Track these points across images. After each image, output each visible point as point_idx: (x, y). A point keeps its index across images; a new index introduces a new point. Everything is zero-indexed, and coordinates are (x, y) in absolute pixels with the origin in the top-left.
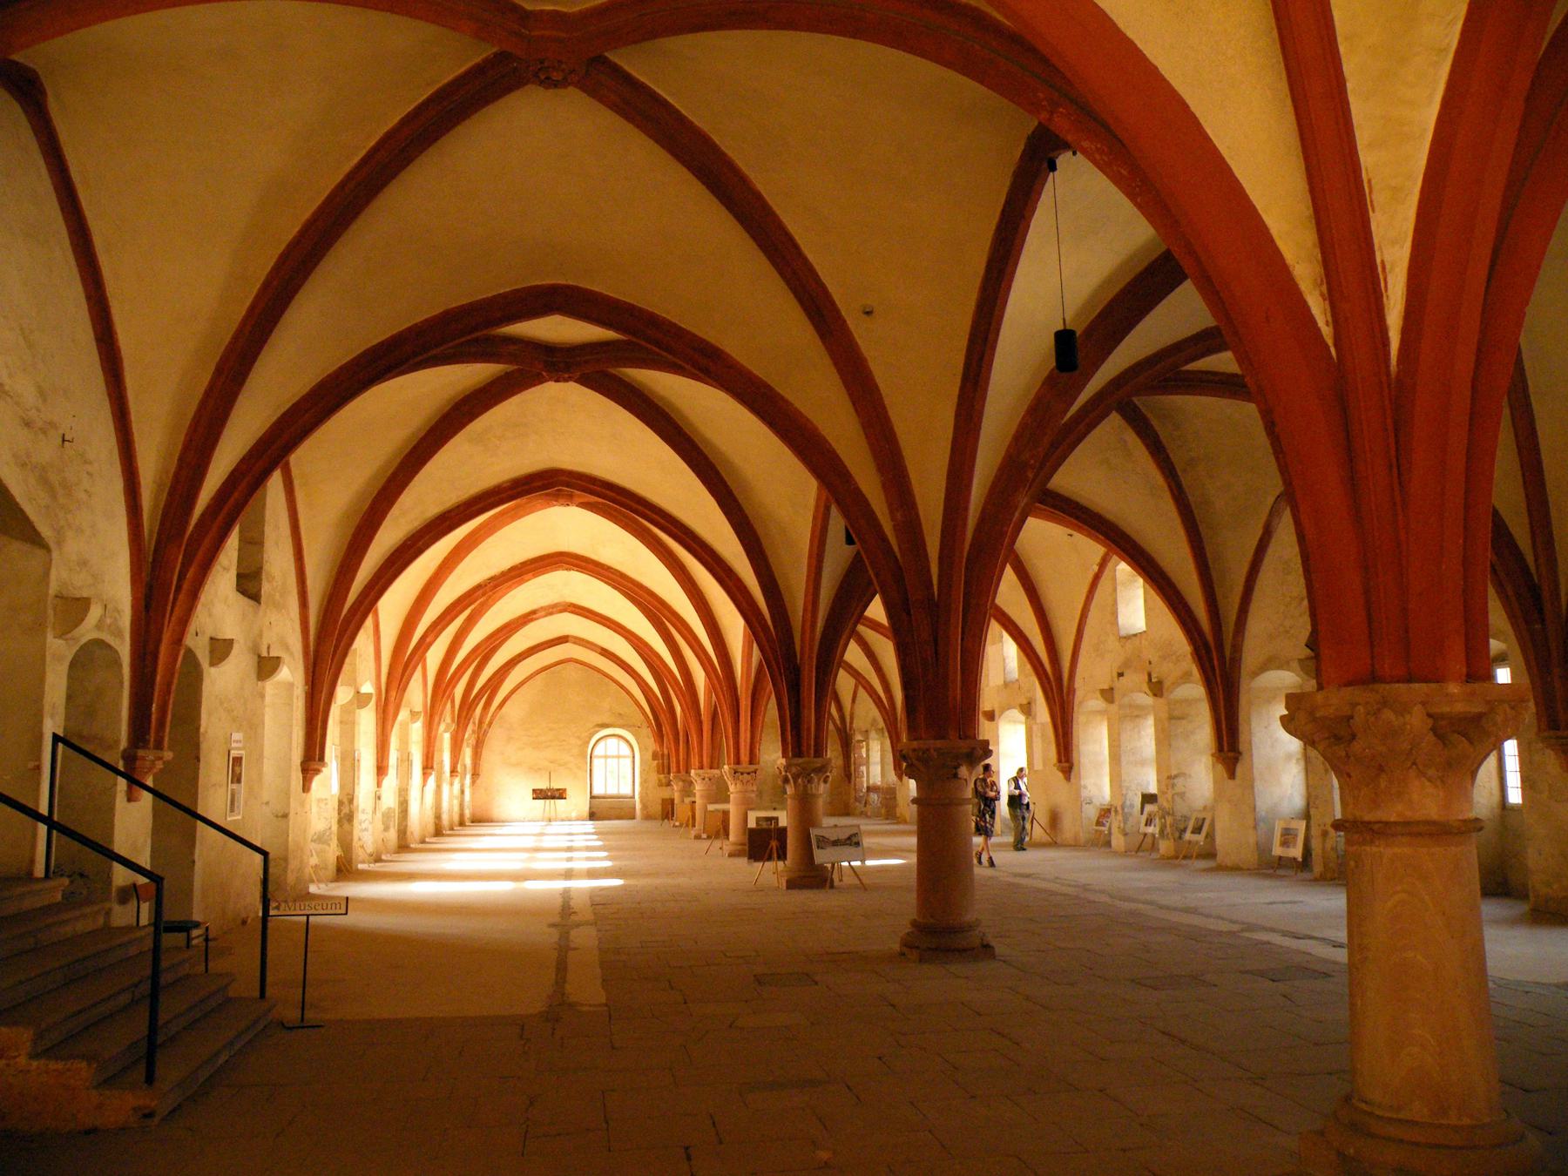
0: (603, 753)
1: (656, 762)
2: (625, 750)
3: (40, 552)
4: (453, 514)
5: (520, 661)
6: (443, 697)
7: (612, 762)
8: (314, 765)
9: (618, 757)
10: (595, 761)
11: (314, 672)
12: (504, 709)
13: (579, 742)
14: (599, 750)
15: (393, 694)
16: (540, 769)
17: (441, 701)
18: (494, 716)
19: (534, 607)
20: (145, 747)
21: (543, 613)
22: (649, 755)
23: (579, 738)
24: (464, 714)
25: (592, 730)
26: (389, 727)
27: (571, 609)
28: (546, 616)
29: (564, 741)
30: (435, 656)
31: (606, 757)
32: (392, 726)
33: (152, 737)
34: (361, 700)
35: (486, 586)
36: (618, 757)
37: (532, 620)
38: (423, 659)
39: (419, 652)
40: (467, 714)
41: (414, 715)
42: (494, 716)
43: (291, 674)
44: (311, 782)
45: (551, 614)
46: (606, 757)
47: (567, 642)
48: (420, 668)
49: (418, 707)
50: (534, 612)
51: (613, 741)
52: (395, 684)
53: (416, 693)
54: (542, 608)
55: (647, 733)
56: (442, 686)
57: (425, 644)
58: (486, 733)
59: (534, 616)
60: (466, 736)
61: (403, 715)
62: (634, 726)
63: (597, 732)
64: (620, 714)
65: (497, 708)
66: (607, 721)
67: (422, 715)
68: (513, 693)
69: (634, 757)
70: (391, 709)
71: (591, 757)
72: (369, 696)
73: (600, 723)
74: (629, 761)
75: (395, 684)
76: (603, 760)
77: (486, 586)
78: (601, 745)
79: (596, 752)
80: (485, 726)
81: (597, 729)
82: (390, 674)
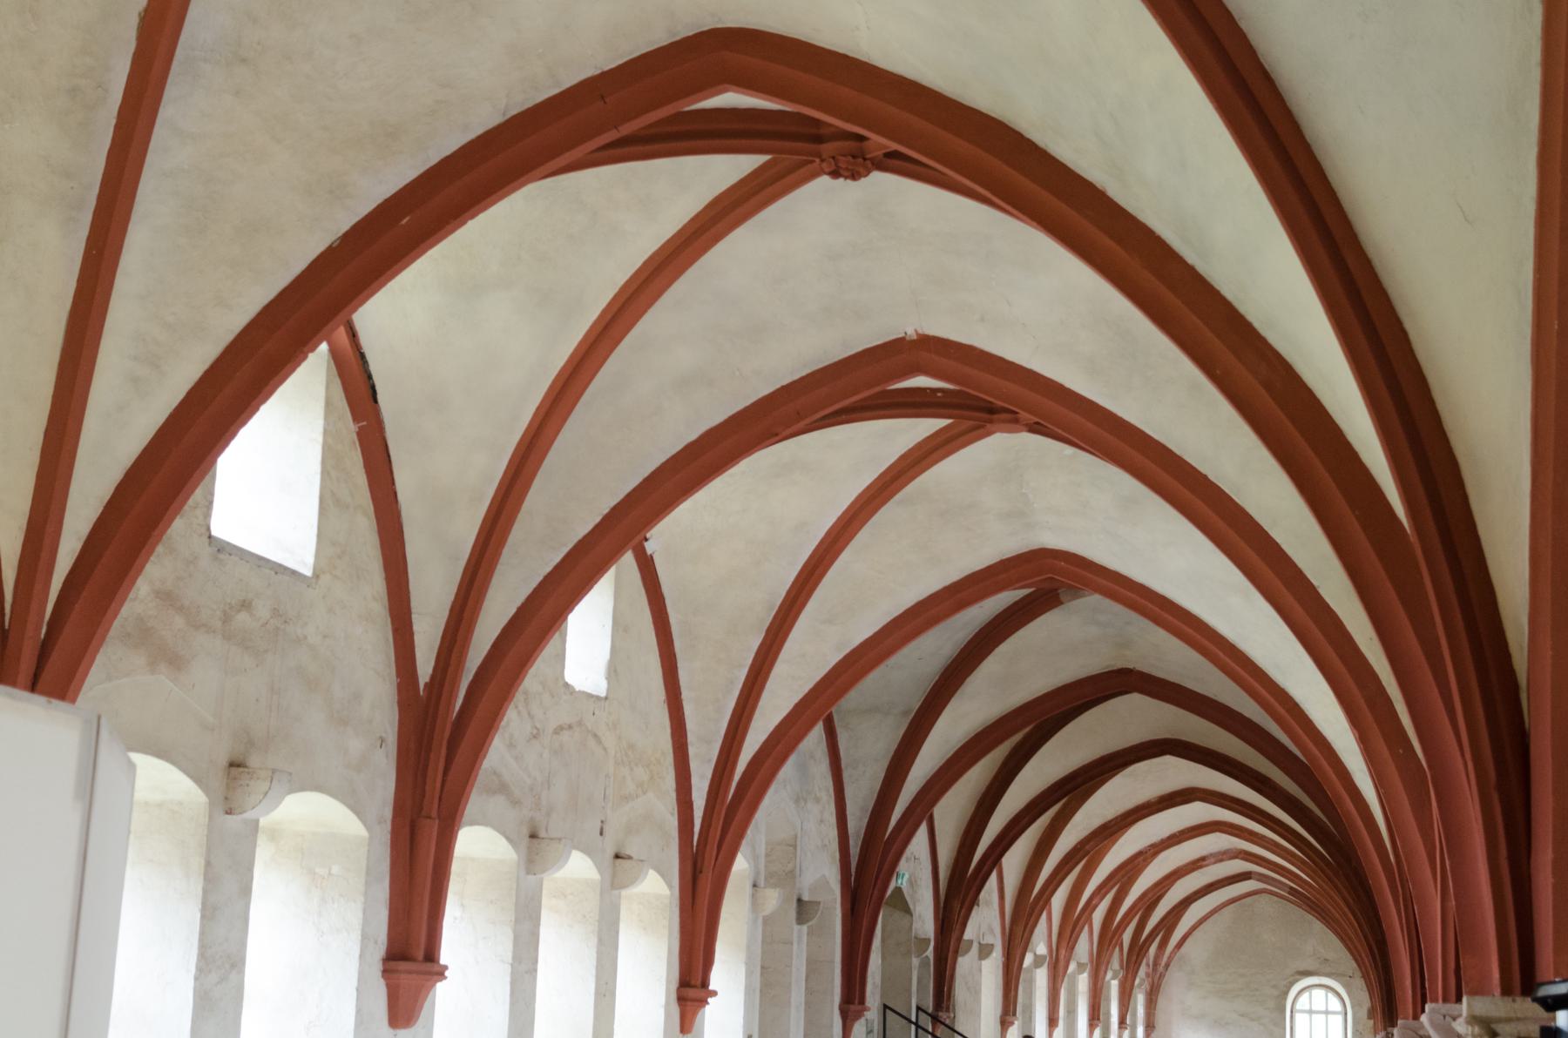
0: (1307, 1007)
1: (1372, 1022)
2: (1335, 1005)
3: (908, 916)
4: (1113, 823)
5: (1196, 900)
6: (1109, 945)
7: (1319, 1019)
8: (1009, 1019)
9: (1327, 1012)
10: (1298, 1016)
11: (1008, 949)
12: (1183, 949)
13: (1276, 993)
14: (1303, 1002)
15: (1063, 952)
16: (1227, 1024)
17: (1107, 950)
18: (1170, 958)
19: (1204, 853)
20: (942, 1011)
21: (1213, 860)
22: (1364, 1012)
23: (1274, 987)
24: (1134, 958)
25: (1291, 979)
26: (1060, 982)
27: (1242, 856)
28: (1215, 863)
29: (1257, 990)
30: (1098, 916)
31: (1311, 1012)
32: (1062, 981)
33: (944, 1005)
34: (1038, 961)
35: (1146, 852)
36: (1327, 1012)
37: (1201, 867)
38: (1089, 921)
39: (1086, 914)
40: (1137, 959)
41: (1081, 967)
42: (1170, 958)
43: (997, 956)
44: (1007, 1030)
45: (1221, 860)
46: (1311, 1012)
47: (1250, 878)
48: (1086, 928)
49: (1085, 958)
50: (1203, 859)
51: (1319, 994)
52: (1064, 944)
53: (1084, 947)
54: (1211, 855)
55: (1359, 983)
56: (1108, 936)
57: (1090, 906)
58: (1162, 976)
59: (1204, 863)
60: (1137, 981)
61: (1072, 967)
62: (1344, 975)
63: (1297, 981)
64: (1326, 960)
65: (1174, 950)
66: (1311, 968)
67: (1089, 966)
68: (1194, 930)
69: (1346, 1014)
70: (1062, 963)
71: (1292, 1012)
72: (1043, 957)
73: (1301, 969)
74: (1340, 1018)
75: (1064, 944)
76: (1306, 1016)
77: (1146, 852)
78: (1306, 995)
79: (1298, 1006)
80: (1161, 969)
81: (1298, 977)
82: (1060, 935)
